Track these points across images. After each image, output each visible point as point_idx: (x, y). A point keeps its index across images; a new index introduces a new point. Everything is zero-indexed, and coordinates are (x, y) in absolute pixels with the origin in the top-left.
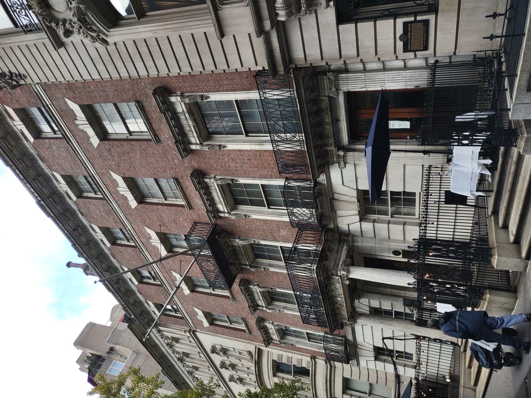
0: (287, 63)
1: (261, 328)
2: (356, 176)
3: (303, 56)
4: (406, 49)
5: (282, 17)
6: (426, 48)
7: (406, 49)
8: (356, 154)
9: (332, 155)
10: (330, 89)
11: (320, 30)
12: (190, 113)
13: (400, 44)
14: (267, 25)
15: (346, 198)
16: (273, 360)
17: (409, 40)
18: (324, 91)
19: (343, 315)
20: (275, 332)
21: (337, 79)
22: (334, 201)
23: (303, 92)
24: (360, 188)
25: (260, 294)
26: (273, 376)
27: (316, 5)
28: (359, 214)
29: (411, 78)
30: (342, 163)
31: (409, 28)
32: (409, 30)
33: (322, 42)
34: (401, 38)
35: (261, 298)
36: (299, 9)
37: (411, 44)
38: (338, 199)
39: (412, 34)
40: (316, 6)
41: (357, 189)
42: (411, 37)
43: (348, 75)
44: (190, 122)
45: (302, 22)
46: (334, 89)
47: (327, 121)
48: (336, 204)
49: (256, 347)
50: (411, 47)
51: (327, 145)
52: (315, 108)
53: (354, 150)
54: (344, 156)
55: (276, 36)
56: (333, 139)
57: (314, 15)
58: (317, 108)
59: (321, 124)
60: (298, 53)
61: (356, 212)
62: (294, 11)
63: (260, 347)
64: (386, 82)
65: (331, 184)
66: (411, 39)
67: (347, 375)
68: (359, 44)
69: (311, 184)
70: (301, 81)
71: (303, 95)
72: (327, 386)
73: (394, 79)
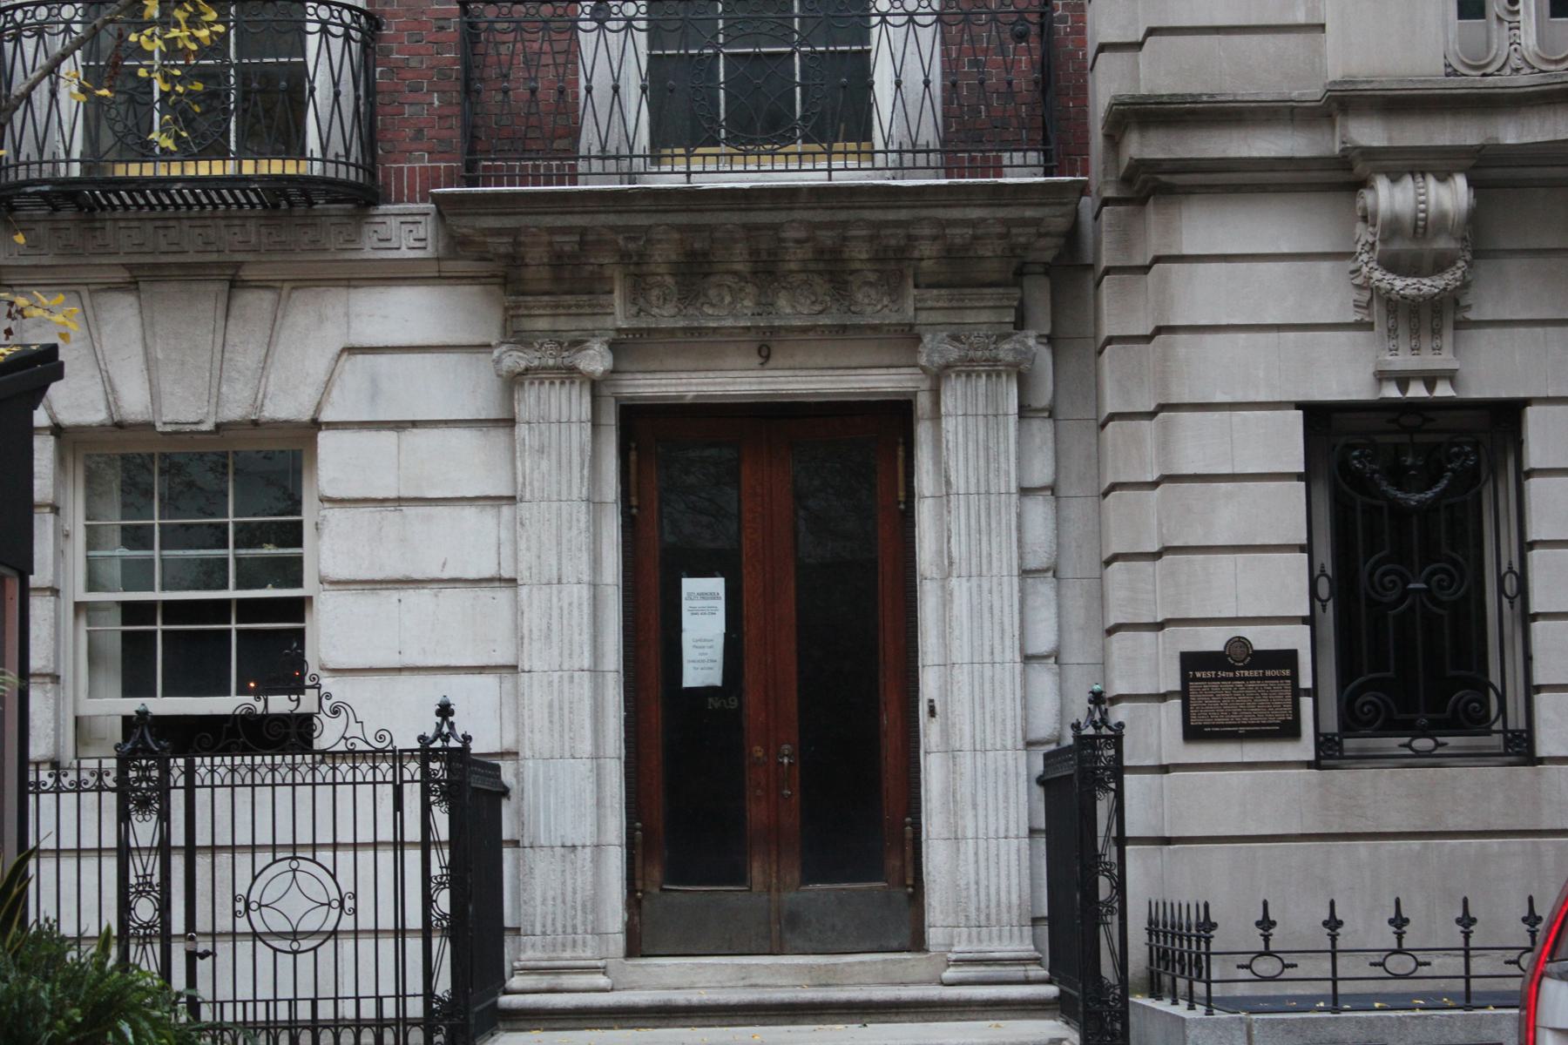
0: (1164, 178)
2: (414, 424)
4: (1192, 663)
6: (1193, 733)
7: (1192, 663)
8: (580, 435)
9: (574, 310)
10: (955, 338)
11: (1291, 335)
13: (1213, 640)
14: (1368, 133)
15: (246, 356)
17: (1231, 675)
18: (940, 304)
21: (994, 369)
22: (226, 286)
23: (975, 213)
24: (325, 439)
27: (1392, 332)
28: (120, 425)
29: (987, 686)
30: (515, 359)
31: (1276, 673)
32: (1268, 673)
33: (1242, 337)
34: (1241, 642)
36: (1392, 265)
37: (1216, 679)
38: (234, 311)
39: (1251, 684)
40: (1389, 330)
41: (316, 425)
42: (1240, 679)
43: (1013, 420)
45: (1325, 267)
46: (953, 353)
47: (783, 303)
48: (206, 300)
50: (1201, 679)
51: (639, 286)
52: (860, 253)
53: (596, 424)
54: (569, 374)
55: (1298, 155)
56: (681, 324)
57: (1352, 317)
58: (857, 266)
61: (135, 404)
62: (1397, 246)
64: (974, 581)
65: (351, 282)
66: (1235, 679)
68: (1223, 486)
69: (347, 164)
70: (1029, 213)
71: (956, 213)
73: (986, 615)
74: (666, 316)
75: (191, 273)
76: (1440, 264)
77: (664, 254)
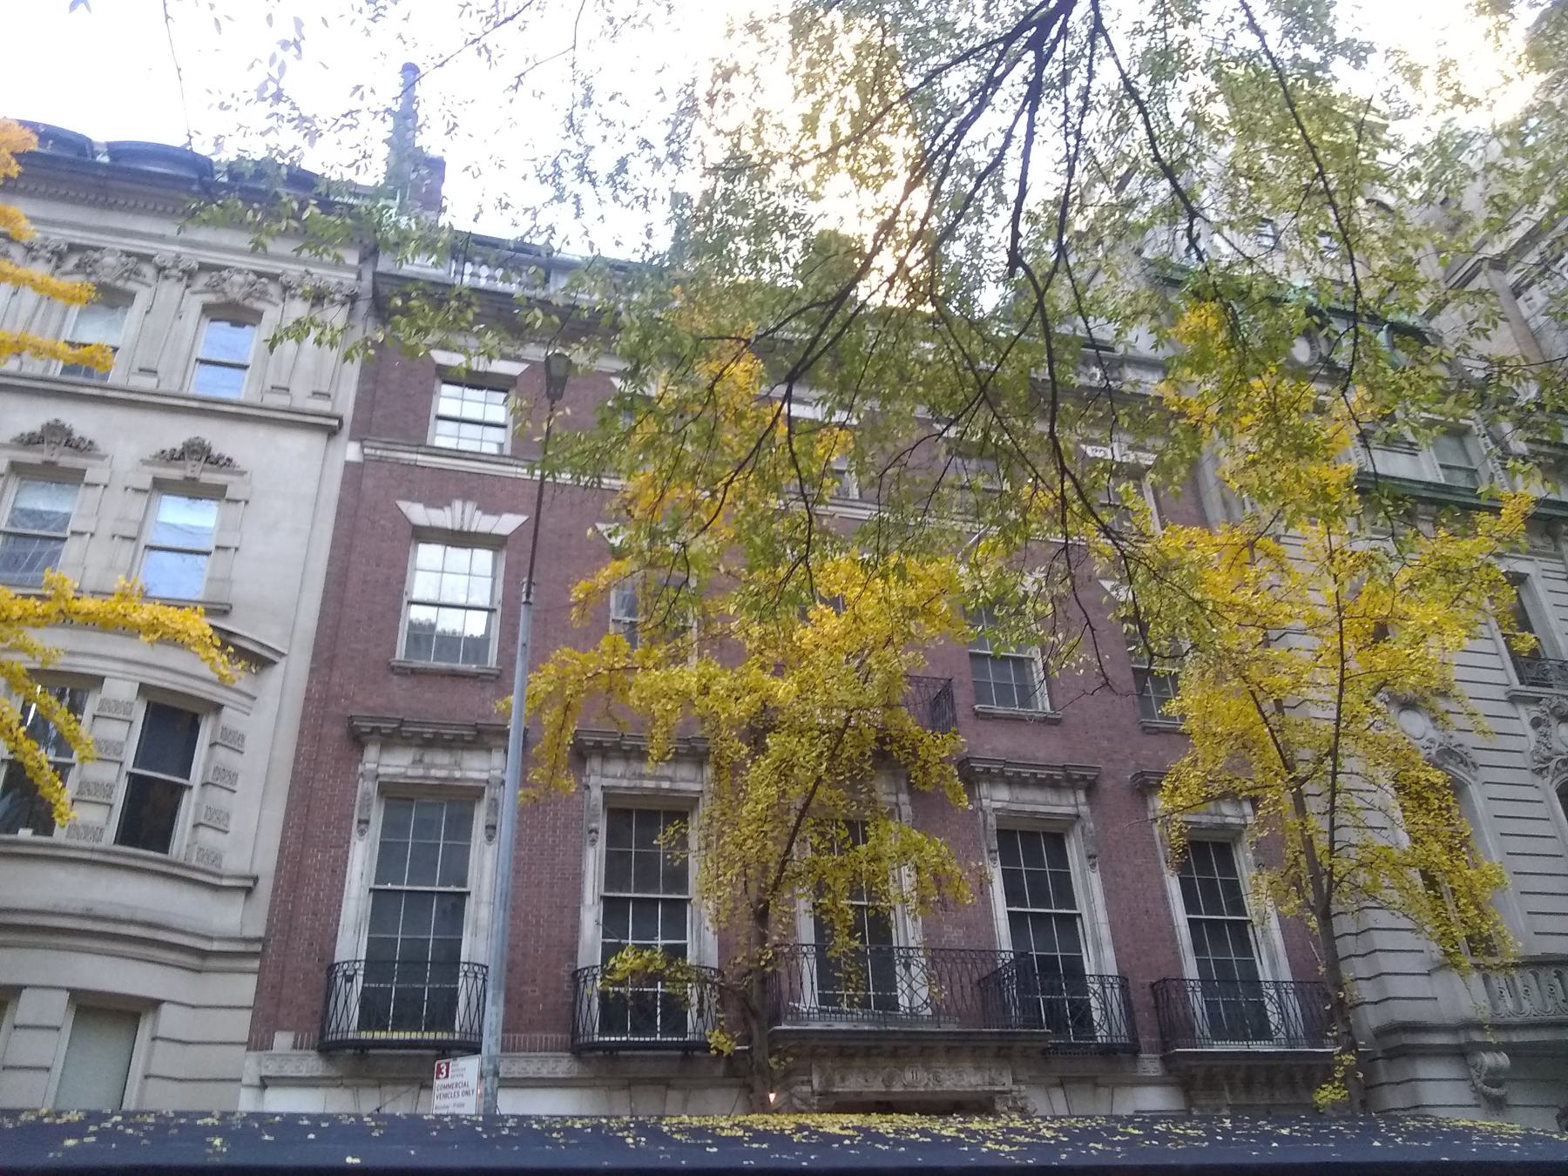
1: (479, 732)
3: (1422, 1076)
5: (1488, 1059)
12: (1224, 827)
14: (1477, 1037)
16: (217, 708)
19: (843, 1079)
20: (434, 772)
25: (666, 785)
26: (142, 686)
35: (650, 784)
44: (1205, 819)
49: (282, 655)
59: (1270, 1083)
60: (1426, 1069)
63: (279, 669)
67: (170, 1021)
72: (131, 922)
74: (1243, 1099)
75: (1081, 1080)
76: (1499, 1085)
77: (1240, 1075)
